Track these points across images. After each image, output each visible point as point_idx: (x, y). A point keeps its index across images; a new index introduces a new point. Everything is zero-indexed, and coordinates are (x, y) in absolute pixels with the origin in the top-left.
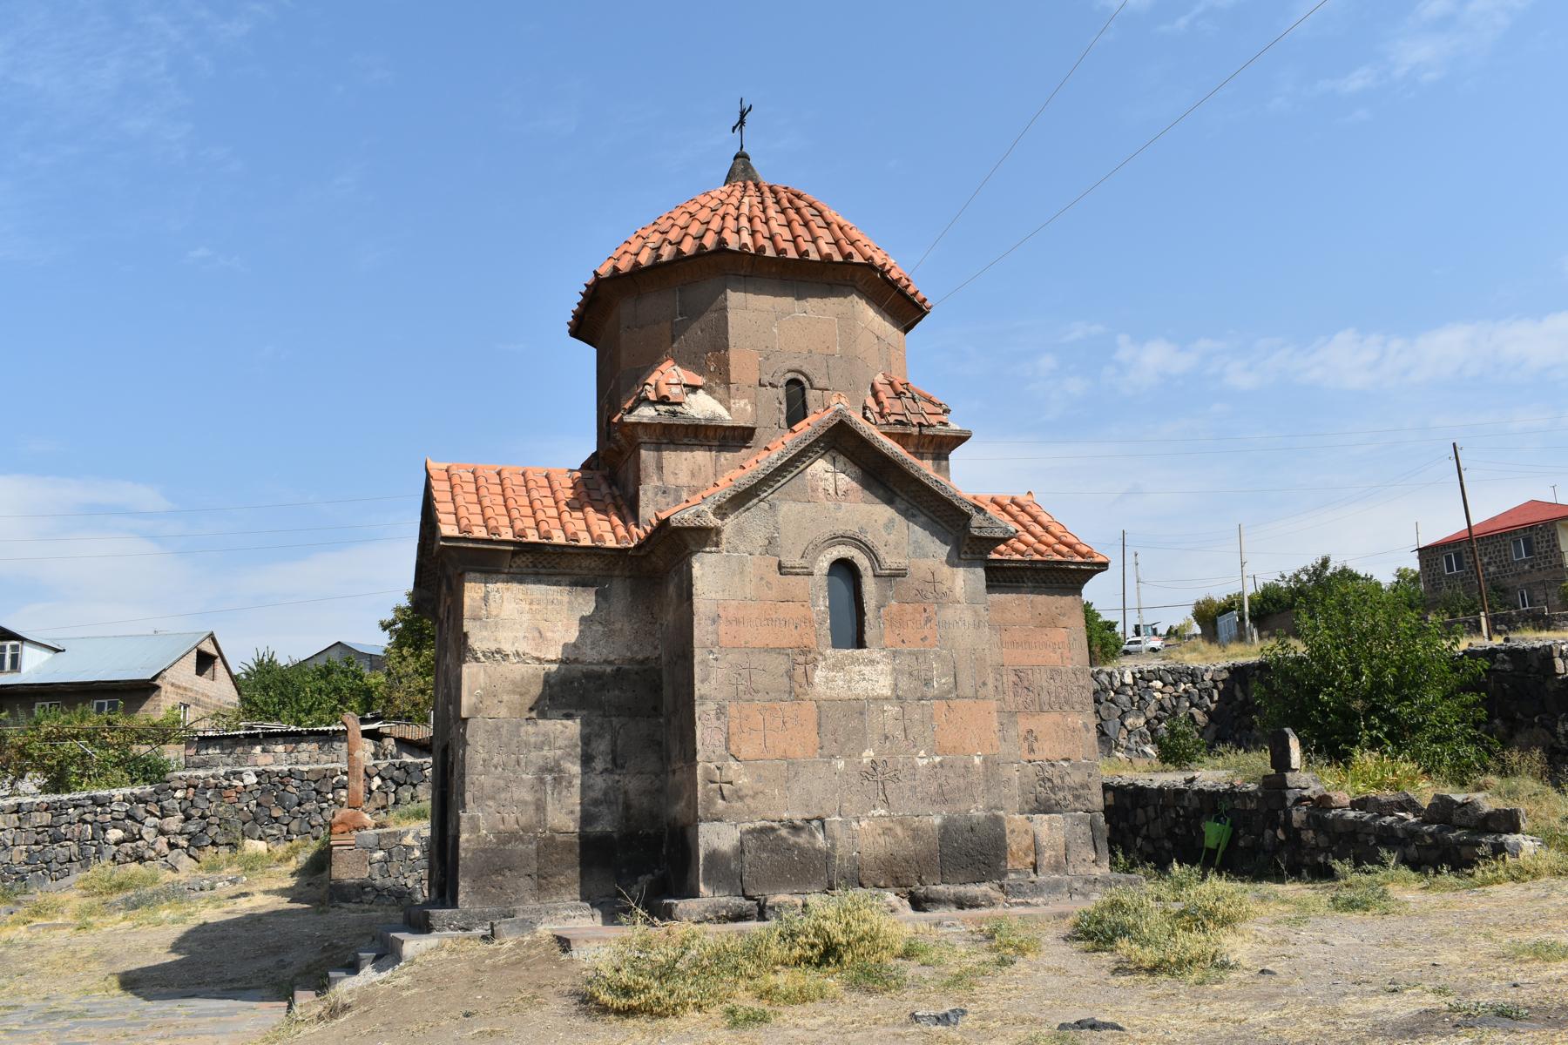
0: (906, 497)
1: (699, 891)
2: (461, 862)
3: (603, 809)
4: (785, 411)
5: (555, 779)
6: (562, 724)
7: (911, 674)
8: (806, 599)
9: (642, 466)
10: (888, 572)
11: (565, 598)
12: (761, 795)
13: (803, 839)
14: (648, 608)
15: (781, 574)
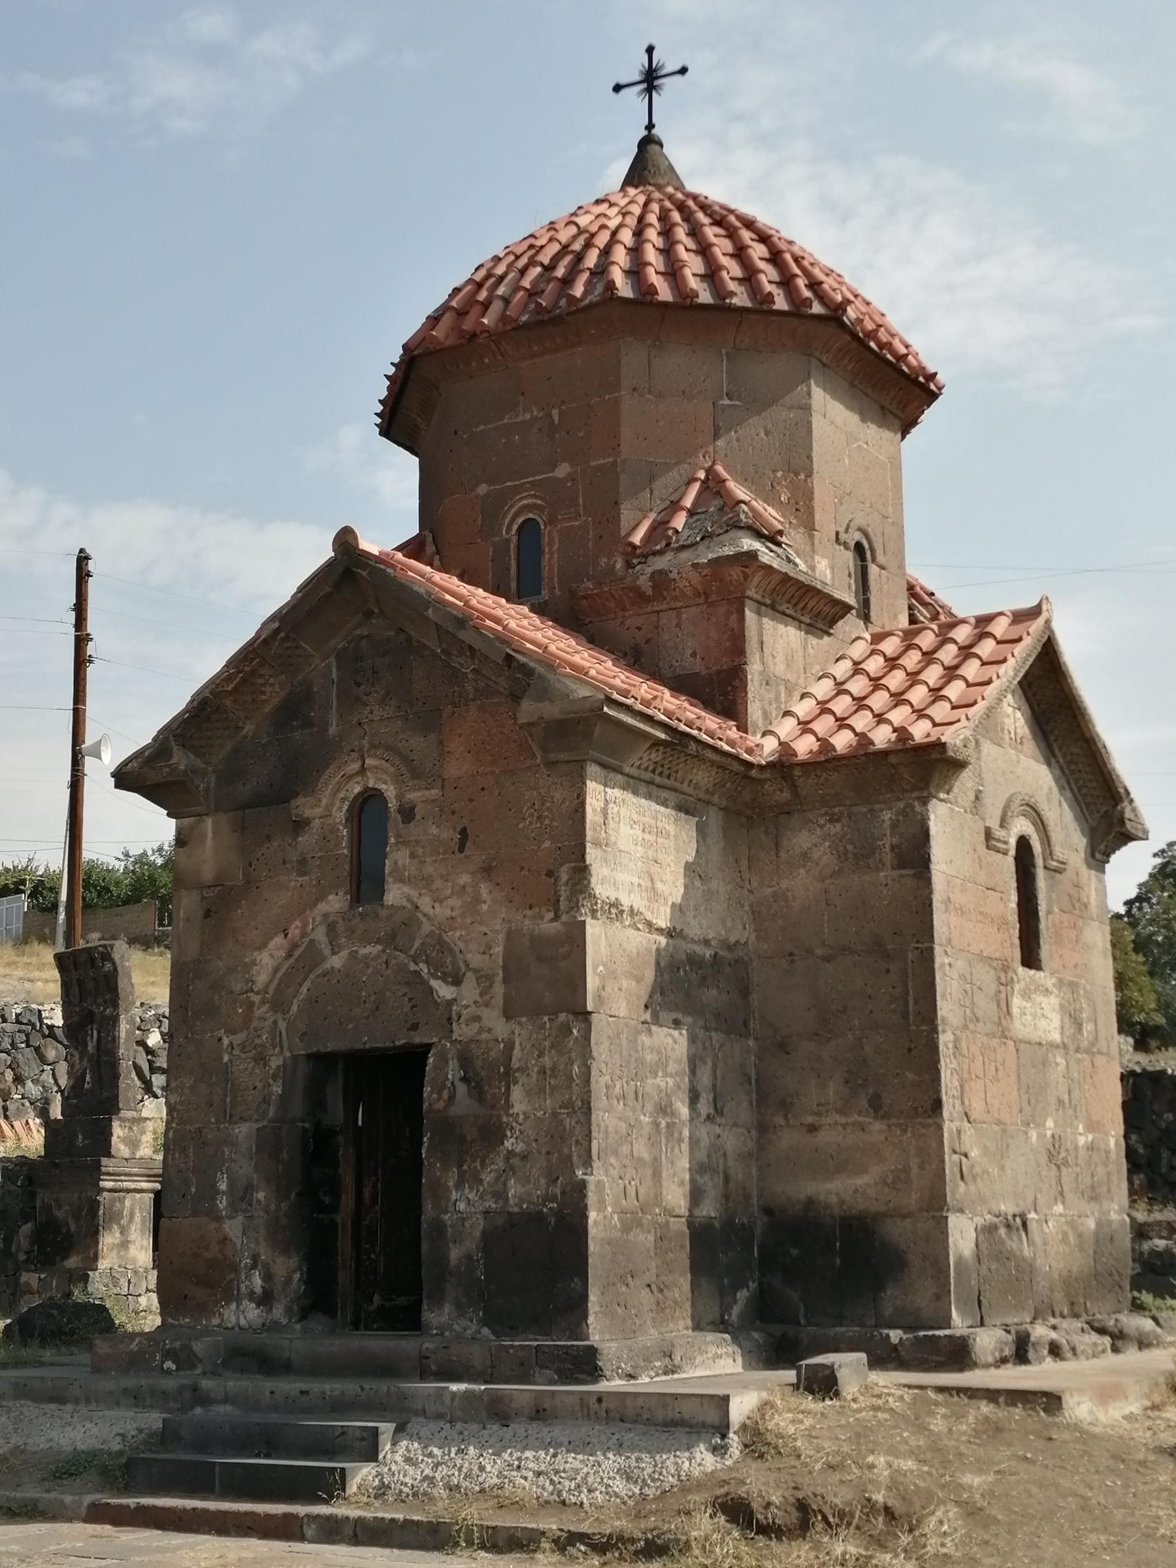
0: (1061, 761)
1: (950, 1317)
2: (590, 1261)
3: (705, 1181)
4: (853, 588)
5: (668, 1126)
6: (672, 1036)
7: (1070, 1015)
8: (1003, 889)
9: (747, 633)
10: (1055, 864)
11: (671, 828)
12: (986, 1176)
13: (1012, 1244)
14: (736, 861)
15: (988, 847)
